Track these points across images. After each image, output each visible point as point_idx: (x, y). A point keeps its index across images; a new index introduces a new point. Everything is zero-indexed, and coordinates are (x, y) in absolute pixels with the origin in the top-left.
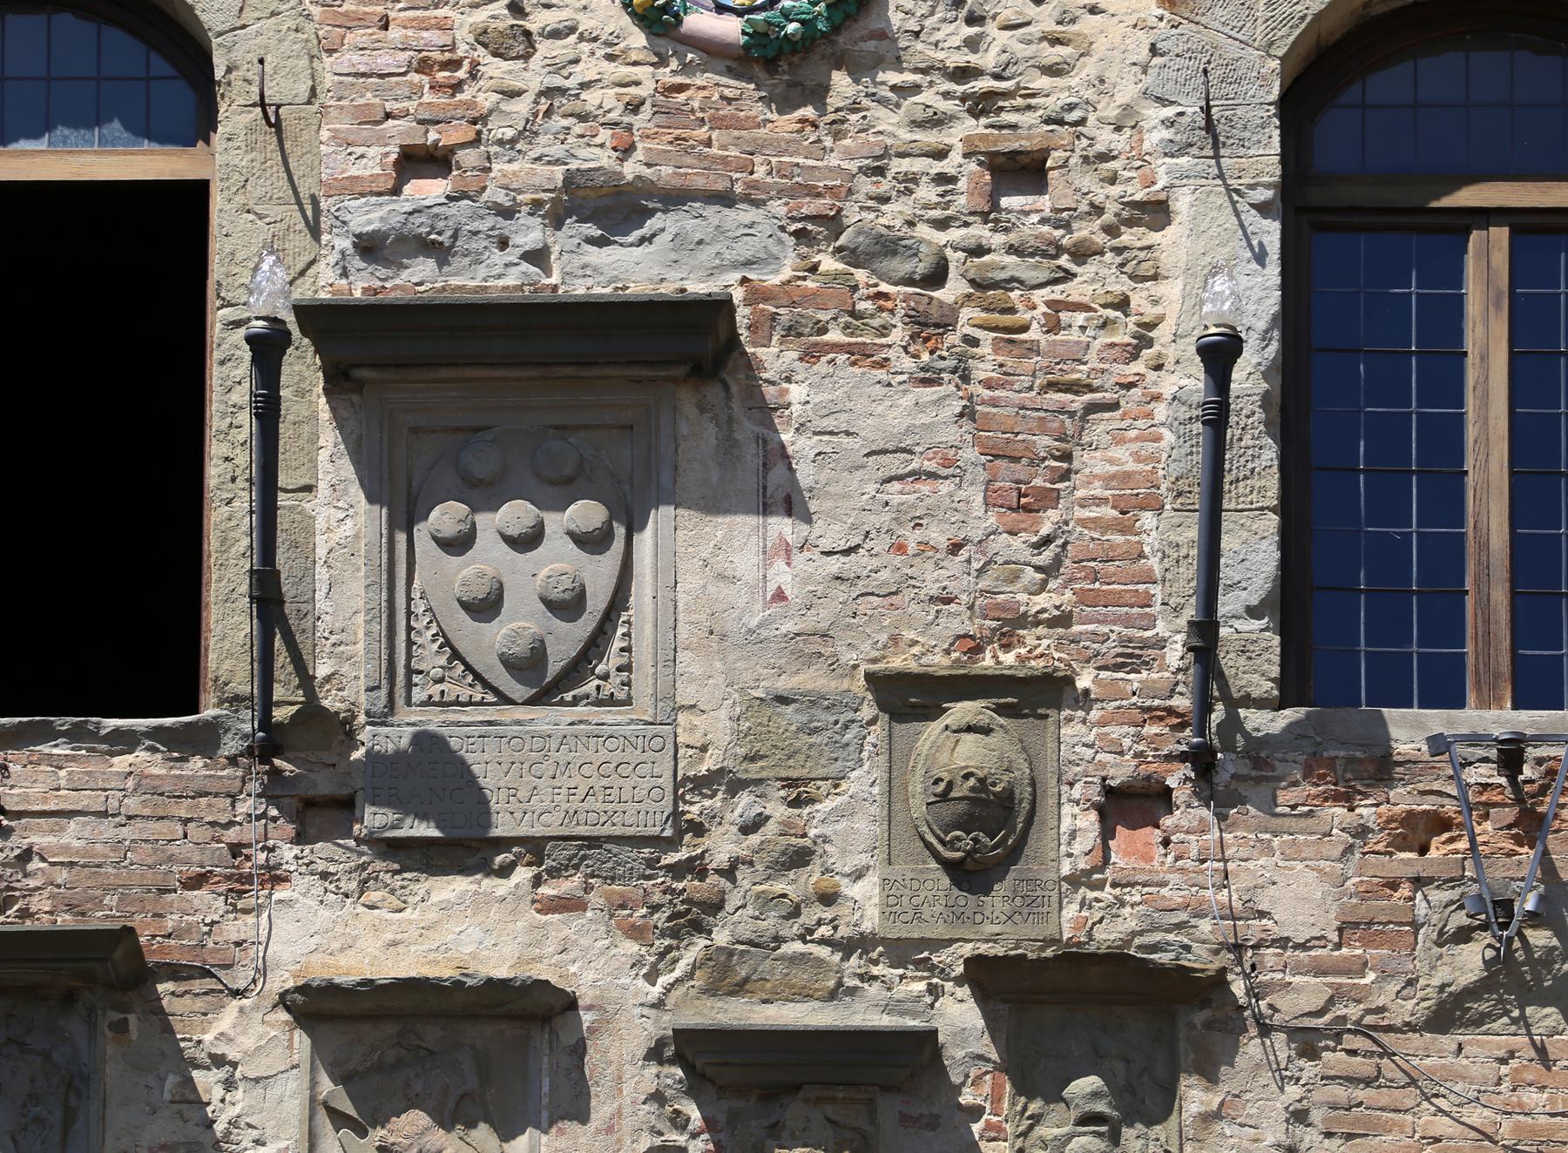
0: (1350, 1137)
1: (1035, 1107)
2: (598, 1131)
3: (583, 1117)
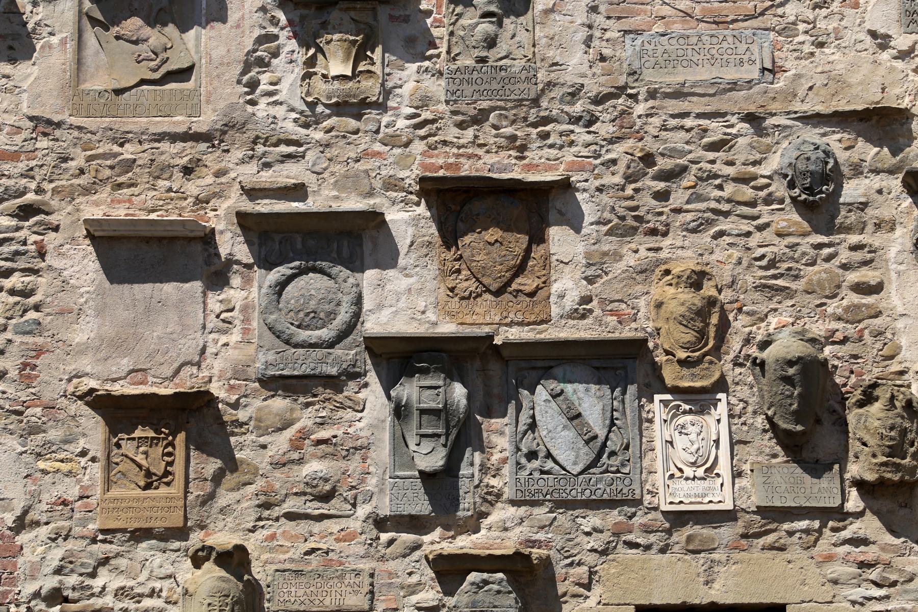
0: (619, 18)
1: (459, 9)
2: (232, 27)
3: (224, 20)
